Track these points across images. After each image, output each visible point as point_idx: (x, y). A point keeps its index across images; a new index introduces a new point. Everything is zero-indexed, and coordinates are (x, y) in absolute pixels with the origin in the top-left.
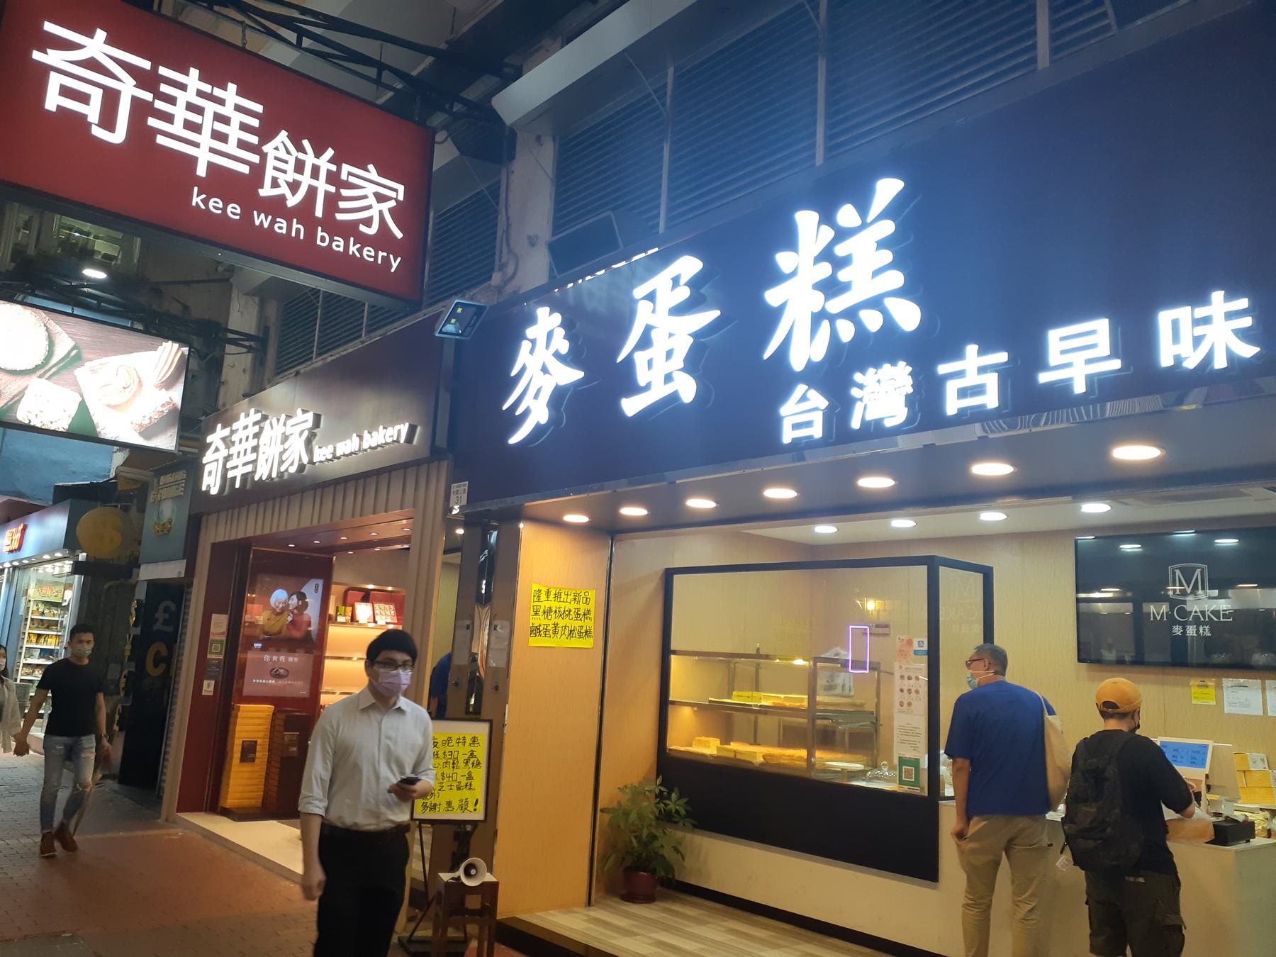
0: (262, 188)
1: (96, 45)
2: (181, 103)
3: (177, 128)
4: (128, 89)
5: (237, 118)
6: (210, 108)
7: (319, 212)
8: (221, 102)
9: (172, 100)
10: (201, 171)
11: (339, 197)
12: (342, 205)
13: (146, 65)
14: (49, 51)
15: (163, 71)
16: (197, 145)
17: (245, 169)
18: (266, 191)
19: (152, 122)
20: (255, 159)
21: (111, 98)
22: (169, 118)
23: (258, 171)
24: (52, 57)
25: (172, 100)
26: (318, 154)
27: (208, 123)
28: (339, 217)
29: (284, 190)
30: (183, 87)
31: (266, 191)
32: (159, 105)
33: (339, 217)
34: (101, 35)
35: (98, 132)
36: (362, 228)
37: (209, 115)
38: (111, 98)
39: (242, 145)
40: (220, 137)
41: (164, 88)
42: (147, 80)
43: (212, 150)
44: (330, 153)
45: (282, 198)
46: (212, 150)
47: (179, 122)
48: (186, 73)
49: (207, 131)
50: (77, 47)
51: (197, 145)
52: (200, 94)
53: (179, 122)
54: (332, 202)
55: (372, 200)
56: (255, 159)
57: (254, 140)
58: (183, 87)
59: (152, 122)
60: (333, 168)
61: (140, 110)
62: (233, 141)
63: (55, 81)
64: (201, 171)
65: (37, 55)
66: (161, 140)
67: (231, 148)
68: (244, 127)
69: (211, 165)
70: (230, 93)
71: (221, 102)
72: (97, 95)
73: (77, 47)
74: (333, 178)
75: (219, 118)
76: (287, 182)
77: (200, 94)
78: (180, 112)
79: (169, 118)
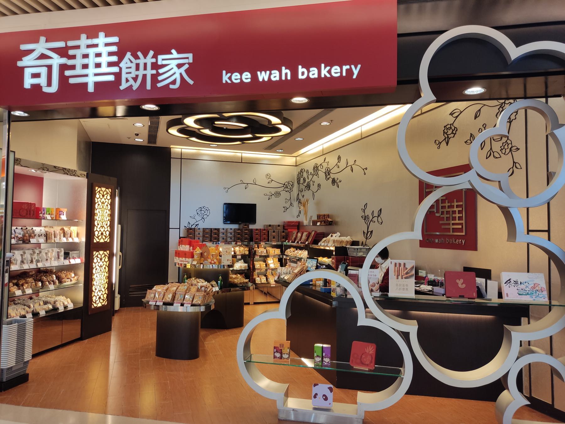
0: (121, 85)
2: (79, 56)
4: (56, 61)
5: (104, 50)
6: (92, 52)
7: (149, 87)
8: (96, 46)
9: (74, 57)
10: (91, 89)
11: (159, 74)
12: (160, 78)
13: (61, 44)
14: (23, 59)
15: (71, 43)
16: (86, 76)
17: (111, 78)
18: (123, 86)
19: (67, 73)
20: (115, 69)
23: (118, 76)
24: (26, 61)
25: (74, 57)
27: (91, 61)
28: (159, 85)
29: (131, 82)
30: (78, 47)
31: (123, 86)
33: (159, 85)
36: (172, 87)
37: (92, 56)
38: (50, 67)
39: (110, 64)
40: (98, 65)
41: (71, 52)
42: (62, 52)
43: (96, 75)
45: (131, 86)
46: (96, 75)
48: (79, 38)
49: (91, 65)
51: (86, 76)
53: (79, 67)
54: (155, 78)
55: (175, 69)
56: (115, 69)
57: (114, 59)
58: (78, 47)
59: (67, 73)
61: (63, 68)
62: (104, 65)
63: (28, 72)
64: (91, 89)
65: (20, 64)
66: (72, 81)
67: (104, 69)
68: (110, 54)
69: (97, 84)
70: (102, 39)
71: (96, 46)
72: (44, 71)
73: (30, 52)
75: (98, 55)
76: (132, 78)
78: (79, 62)
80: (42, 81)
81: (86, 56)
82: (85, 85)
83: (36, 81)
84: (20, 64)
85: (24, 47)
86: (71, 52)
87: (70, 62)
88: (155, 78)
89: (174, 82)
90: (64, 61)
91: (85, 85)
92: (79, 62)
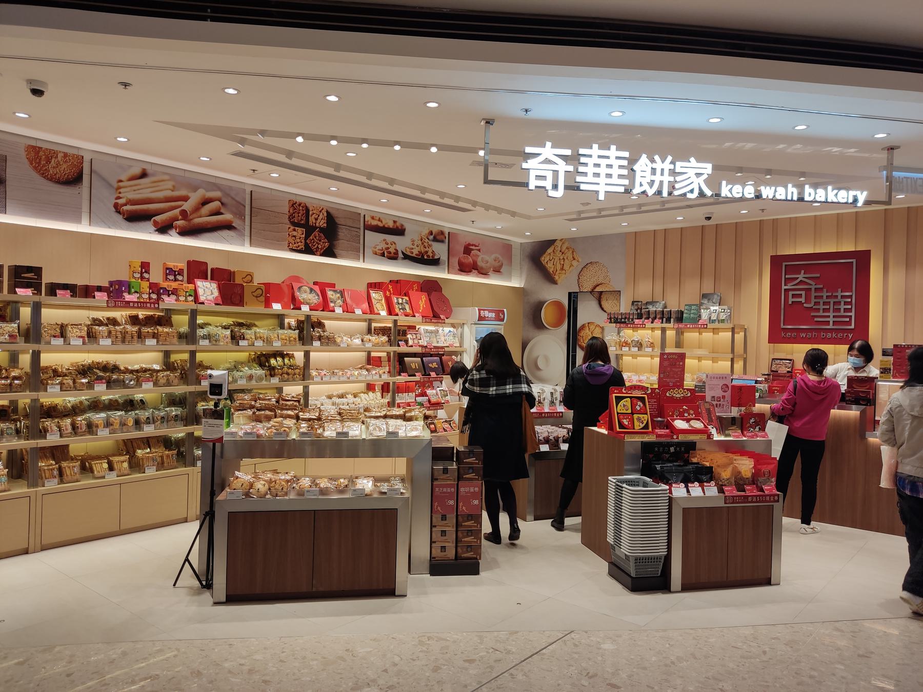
1: (548, 151)
3: (590, 178)
9: (586, 164)
14: (528, 161)
21: (556, 173)
22: (585, 174)
24: (530, 164)
26: (663, 162)
32: (581, 169)
34: (549, 144)
35: (552, 193)
38: (556, 173)
41: (583, 160)
44: (670, 158)
47: (590, 175)
48: (591, 148)
50: (537, 155)
52: (599, 157)
53: (590, 175)
60: (672, 167)
72: (550, 176)
73: (539, 154)
74: (673, 173)
77: (599, 157)
78: (590, 170)
79: (585, 174)
80: (548, 184)
81: (597, 165)
82: (597, 192)
83: (541, 183)
84: (525, 166)
85: (528, 150)
86: (583, 160)
87: (581, 169)
88: (672, 187)
89: (692, 191)
90: (571, 168)
91: (597, 192)
92: (590, 170)
